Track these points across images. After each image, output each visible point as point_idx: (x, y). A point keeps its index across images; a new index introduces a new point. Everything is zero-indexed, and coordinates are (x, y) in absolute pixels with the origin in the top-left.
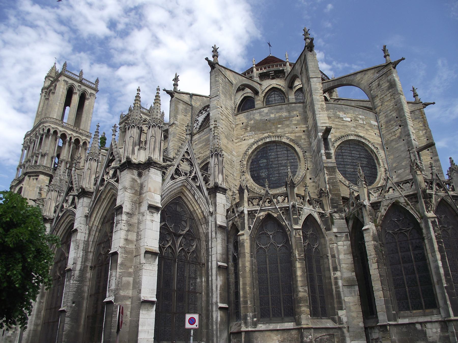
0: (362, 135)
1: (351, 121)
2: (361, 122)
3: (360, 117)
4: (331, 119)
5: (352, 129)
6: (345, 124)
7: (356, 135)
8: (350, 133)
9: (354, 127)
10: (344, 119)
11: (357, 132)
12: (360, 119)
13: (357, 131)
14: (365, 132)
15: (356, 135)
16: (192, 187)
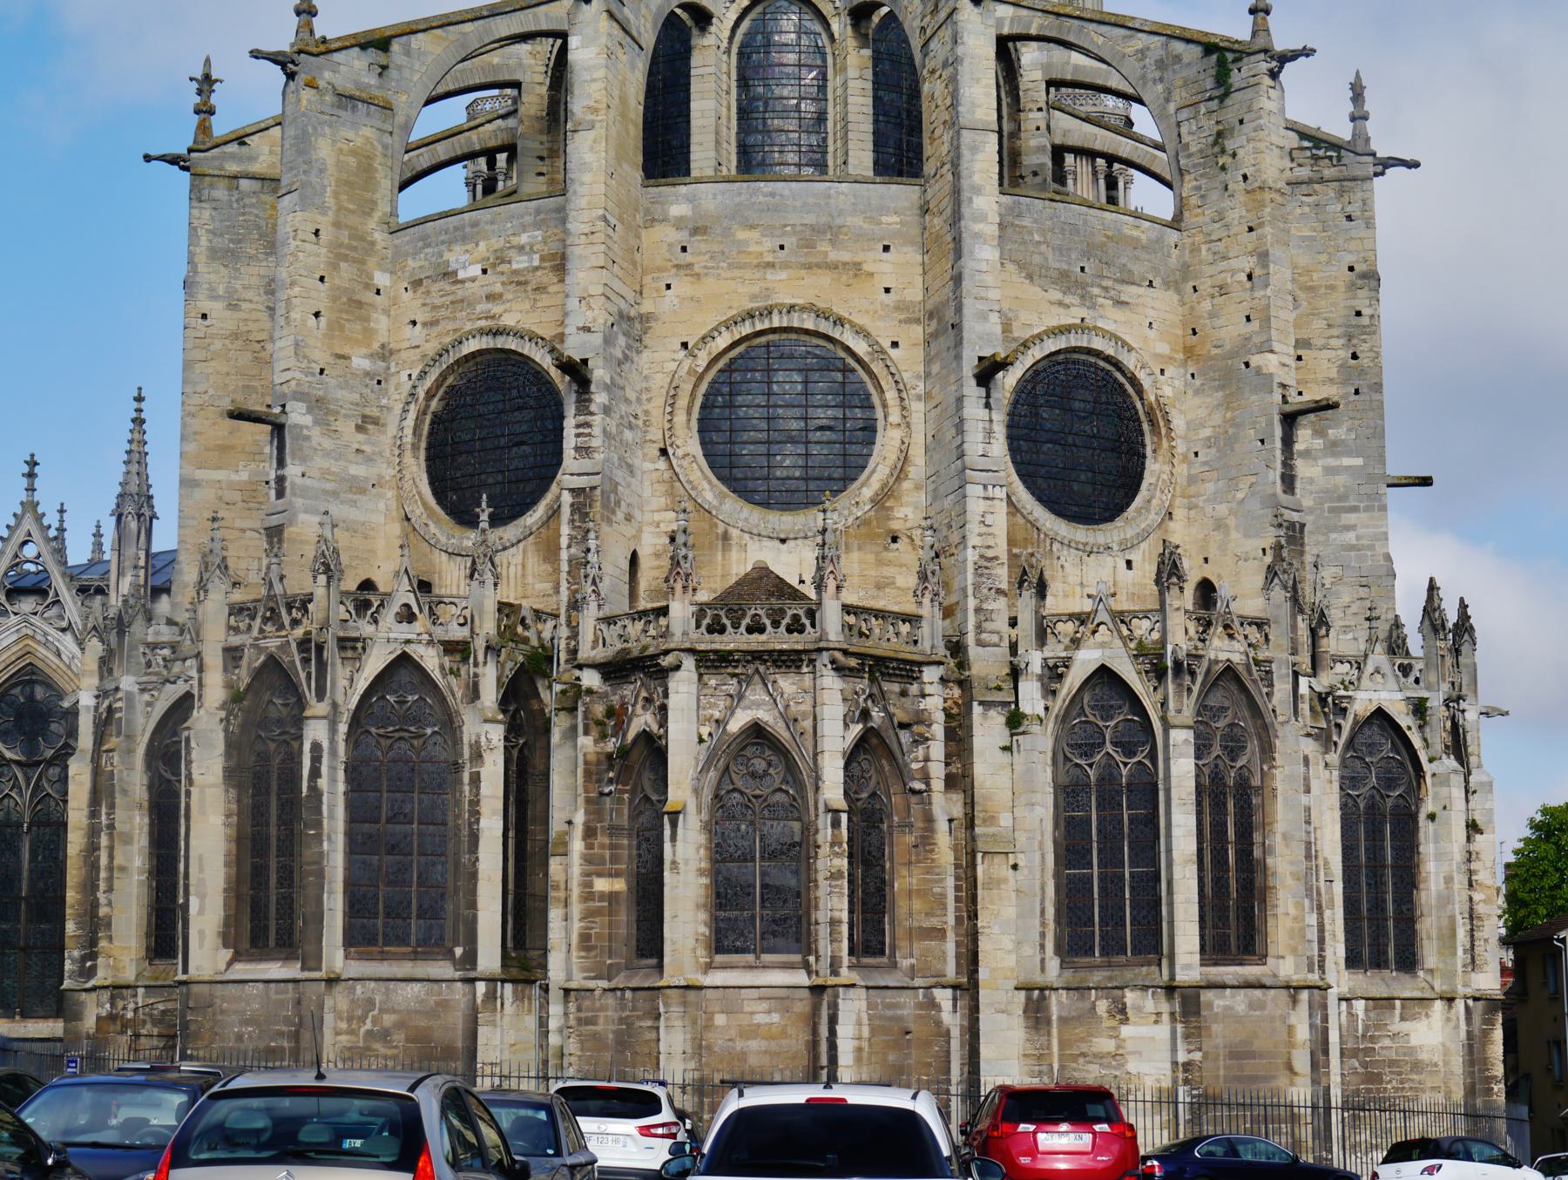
0: (509, 321)
1: (484, 271)
2: (520, 263)
3: (524, 239)
4: (422, 289)
5: (479, 308)
6: (460, 294)
7: (483, 332)
8: (468, 327)
9: (490, 297)
10: (461, 275)
11: (493, 317)
12: (521, 248)
13: (496, 309)
14: (527, 305)
15: (483, 332)
16: (45, 634)
